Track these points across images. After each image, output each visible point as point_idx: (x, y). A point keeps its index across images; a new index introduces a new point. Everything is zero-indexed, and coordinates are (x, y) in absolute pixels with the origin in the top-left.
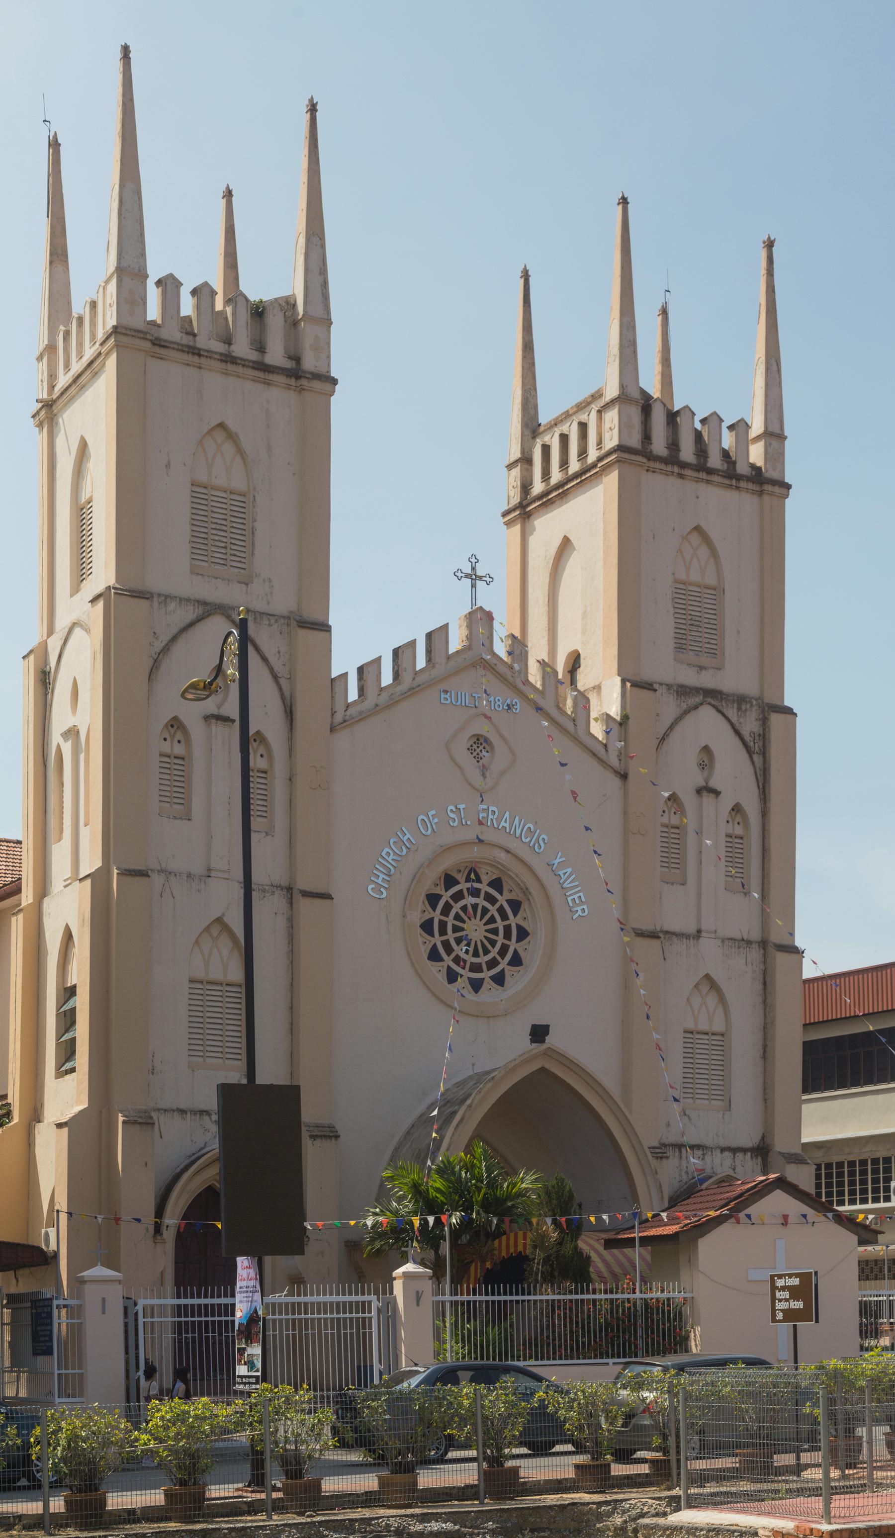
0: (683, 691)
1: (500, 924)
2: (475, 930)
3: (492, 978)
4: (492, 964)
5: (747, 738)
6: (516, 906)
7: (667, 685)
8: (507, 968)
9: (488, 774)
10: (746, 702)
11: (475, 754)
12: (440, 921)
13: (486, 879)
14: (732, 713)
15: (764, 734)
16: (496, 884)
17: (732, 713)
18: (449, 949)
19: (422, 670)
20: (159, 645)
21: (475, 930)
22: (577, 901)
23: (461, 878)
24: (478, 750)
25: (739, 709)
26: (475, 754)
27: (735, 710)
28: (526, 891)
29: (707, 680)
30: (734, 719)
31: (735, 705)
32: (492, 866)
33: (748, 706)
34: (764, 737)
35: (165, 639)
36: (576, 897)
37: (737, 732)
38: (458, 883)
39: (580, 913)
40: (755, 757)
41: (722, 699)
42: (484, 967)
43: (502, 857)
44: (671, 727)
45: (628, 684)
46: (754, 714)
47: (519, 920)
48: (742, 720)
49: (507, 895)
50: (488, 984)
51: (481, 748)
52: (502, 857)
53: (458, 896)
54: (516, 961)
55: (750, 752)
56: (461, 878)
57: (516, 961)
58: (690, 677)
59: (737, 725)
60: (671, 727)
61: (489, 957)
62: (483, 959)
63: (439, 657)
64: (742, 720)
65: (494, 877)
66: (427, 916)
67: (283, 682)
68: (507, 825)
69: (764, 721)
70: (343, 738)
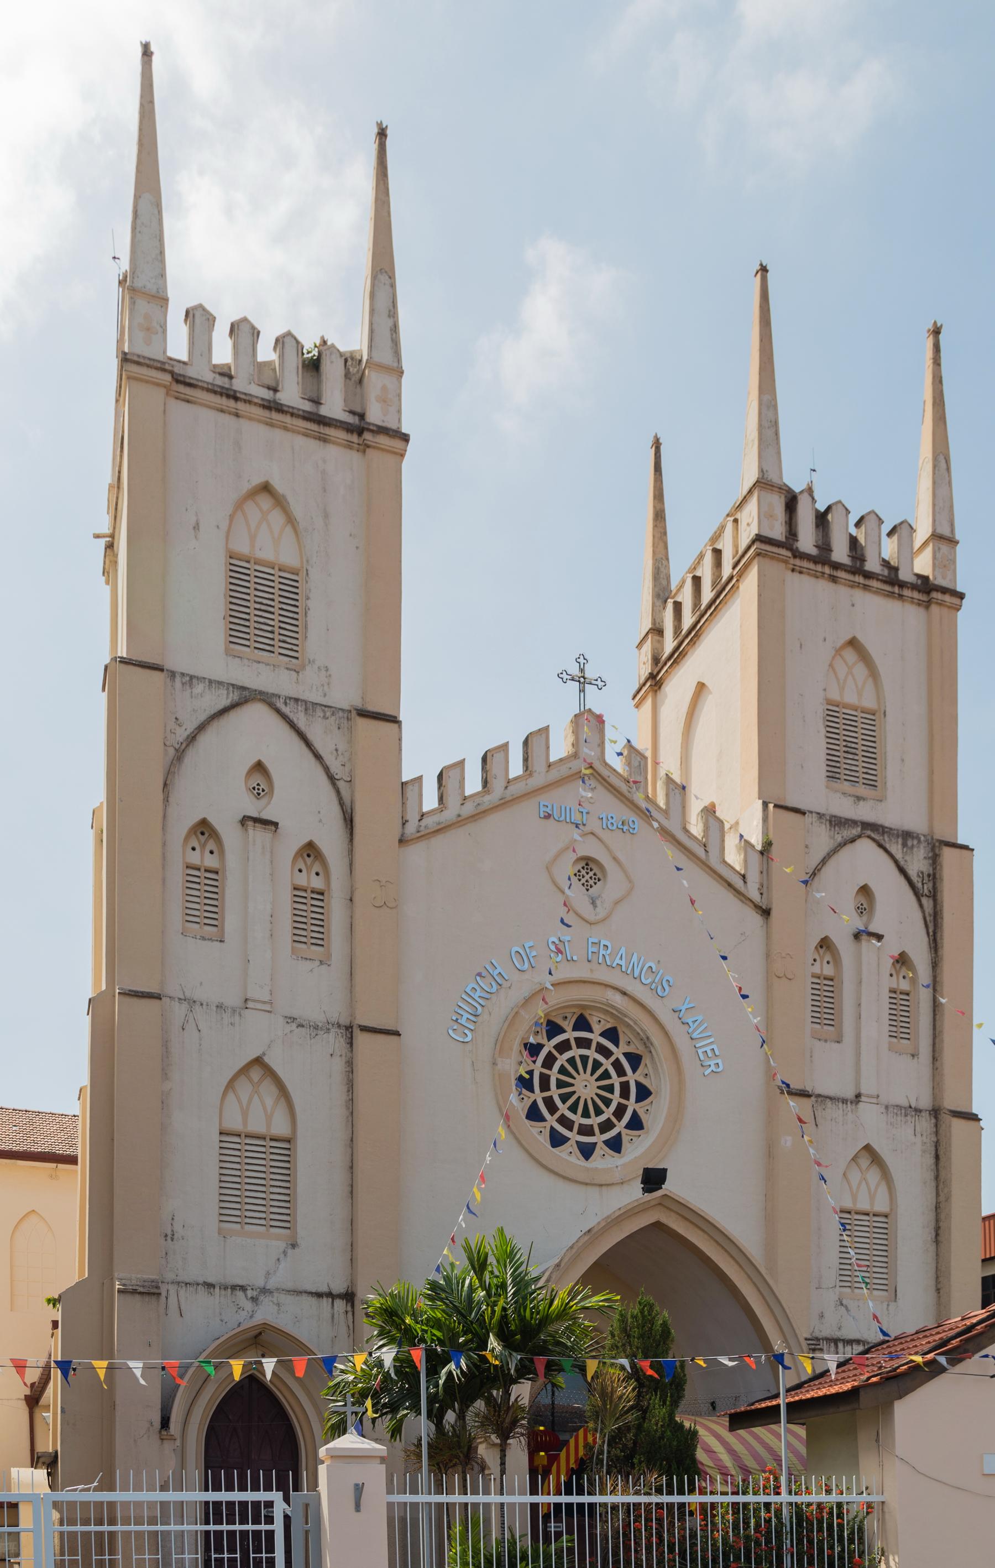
0: (837, 822)
1: (616, 1081)
3: (606, 1143)
4: (606, 1126)
5: (915, 878)
6: (635, 1060)
7: (818, 813)
8: (625, 1132)
9: (598, 902)
10: (913, 838)
11: (583, 881)
13: (598, 1029)
14: (896, 849)
15: (934, 874)
16: (611, 1034)
17: (896, 849)
19: (516, 779)
20: (182, 734)
22: (710, 1054)
23: (568, 1025)
24: (587, 877)
25: (904, 845)
26: (583, 881)
27: (900, 846)
28: (646, 1042)
29: (865, 812)
30: (899, 856)
31: (900, 840)
32: (606, 1012)
33: (915, 842)
34: (934, 878)
35: (190, 726)
36: (708, 1049)
37: (902, 871)
38: (563, 1031)
39: (713, 1068)
40: (924, 901)
41: (883, 833)
42: (597, 1130)
43: (617, 1000)
44: (824, 861)
45: (771, 806)
46: (922, 851)
47: (639, 1076)
48: (907, 858)
49: (624, 1048)
50: (601, 1149)
51: (591, 874)
52: (617, 1000)
53: (564, 1047)
54: (636, 1124)
55: (918, 895)
56: (568, 1025)
57: (636, 1124)
58: (845, 808)
59: (902, 863)
60: (824, 861)
62: (594, 1121)
63: (538, 765)
64: (907, 858)
65: (609, 1026)
67: (341, 784)
68: (623, 963)
69: (935, 859)
70: (416, 854)
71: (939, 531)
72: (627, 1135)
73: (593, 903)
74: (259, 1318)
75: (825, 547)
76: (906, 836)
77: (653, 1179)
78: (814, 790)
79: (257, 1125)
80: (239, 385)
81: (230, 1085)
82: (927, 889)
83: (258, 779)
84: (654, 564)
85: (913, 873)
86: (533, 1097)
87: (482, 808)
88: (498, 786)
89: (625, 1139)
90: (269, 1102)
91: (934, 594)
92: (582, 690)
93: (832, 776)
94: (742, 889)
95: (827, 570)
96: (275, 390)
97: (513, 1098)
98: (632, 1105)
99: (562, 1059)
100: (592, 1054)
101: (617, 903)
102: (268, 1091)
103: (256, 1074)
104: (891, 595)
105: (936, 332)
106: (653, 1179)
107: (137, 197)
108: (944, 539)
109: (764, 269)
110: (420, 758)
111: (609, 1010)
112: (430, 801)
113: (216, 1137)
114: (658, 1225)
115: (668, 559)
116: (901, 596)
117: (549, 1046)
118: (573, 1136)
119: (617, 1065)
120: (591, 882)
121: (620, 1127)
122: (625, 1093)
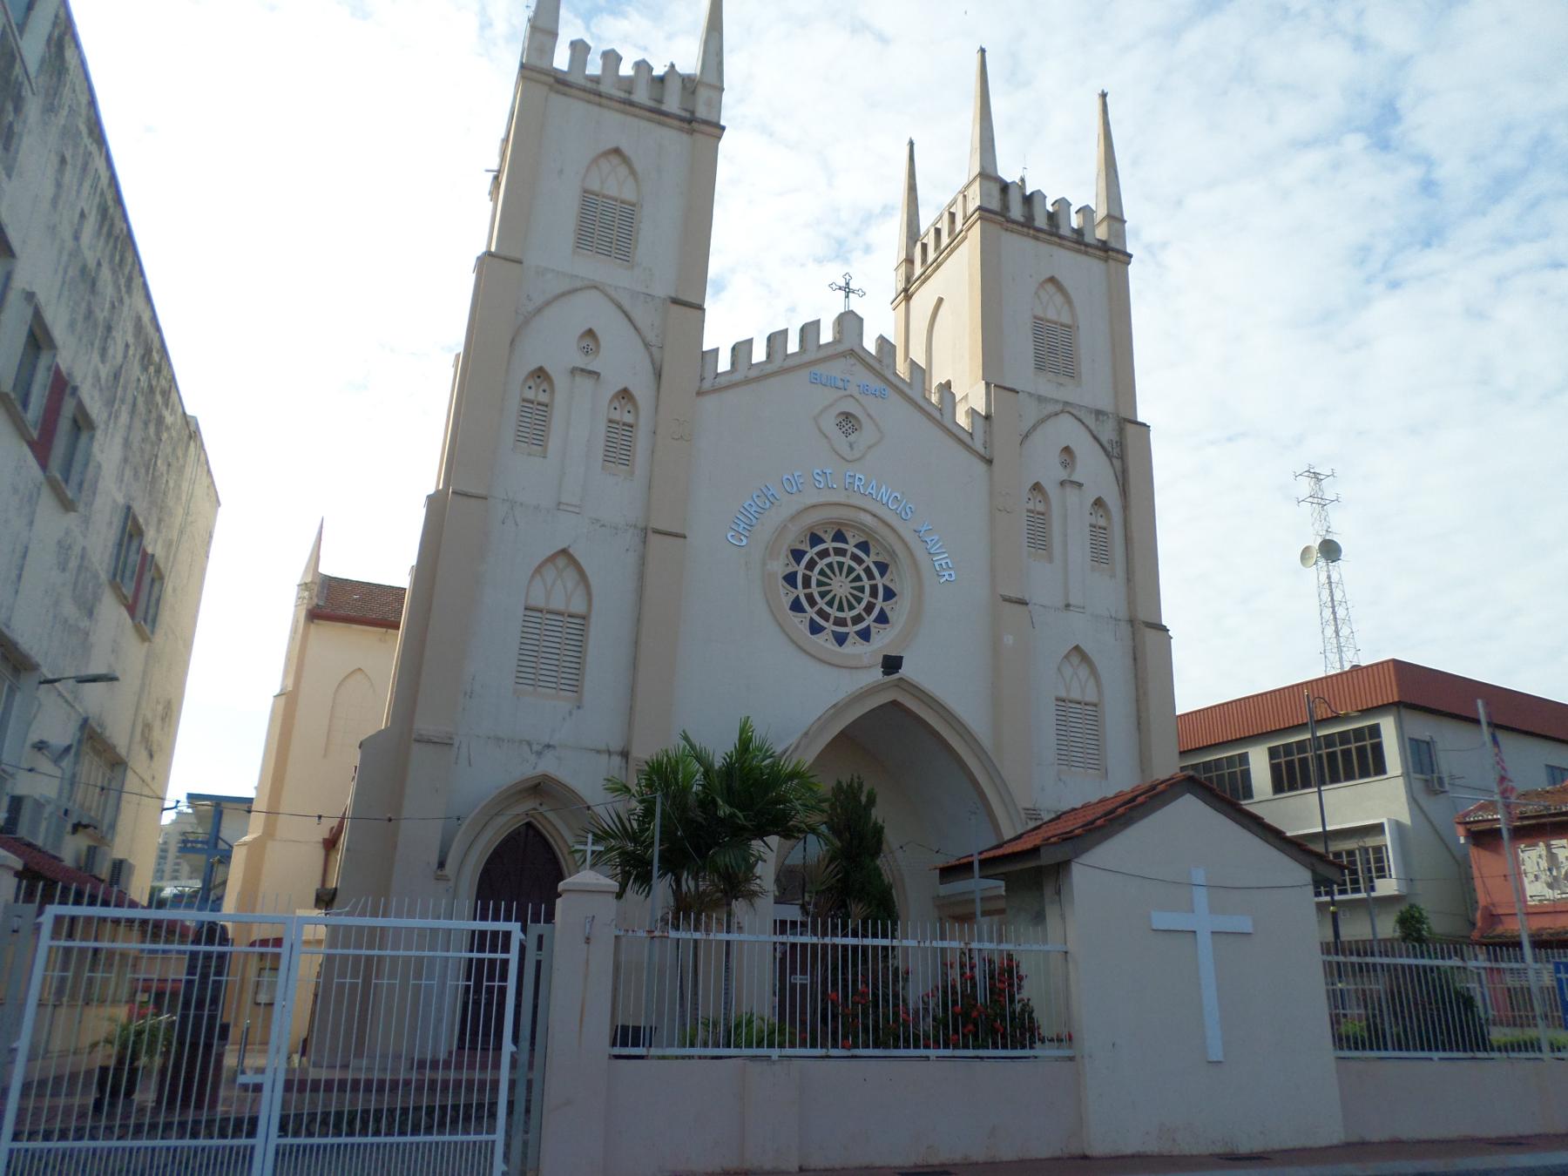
1: (866, 583)
2: (841, 587)
3: (858, 633)
4: (858, 619)
6: (883, 568)
12: (805, 576)
16: (864, 546)
23: (828, 537)
28: (893, 554)
30: (1093, 427)
37: (1096, 438)
44: (1034, 427)
47: (886, 580)
49: (873, 557)
50: (853, 638)
52: (868, 519)
53: (824, 554)
54: (883, 619)
56: (828, 537)
57: (883, 619)
60: (1034, 427)
66: (790, 569)
69: (1121, 431)
70: (710, 402)
73: (851, 446)
74: (540, 770)
76: (1099, 413)
77: (892, 664)
79: (558, 603)
80: (603, 88)
81: (539, 570)
82: (1116, 452)
83: (588, 341)
85: (1104, 440)
86: (796, 592)
90: (570, 585)
93: (1040, 367)
96: (630, 93)
97: (782, 592)
98: (879, 603)
101: (870, 447)
102: (571, 576)
103: (561, 562)
111: (861, 527)
113: (520, 612)
117: (811, 553)
118: (829, 626)
119: (868, 571)
122: (874, 593)
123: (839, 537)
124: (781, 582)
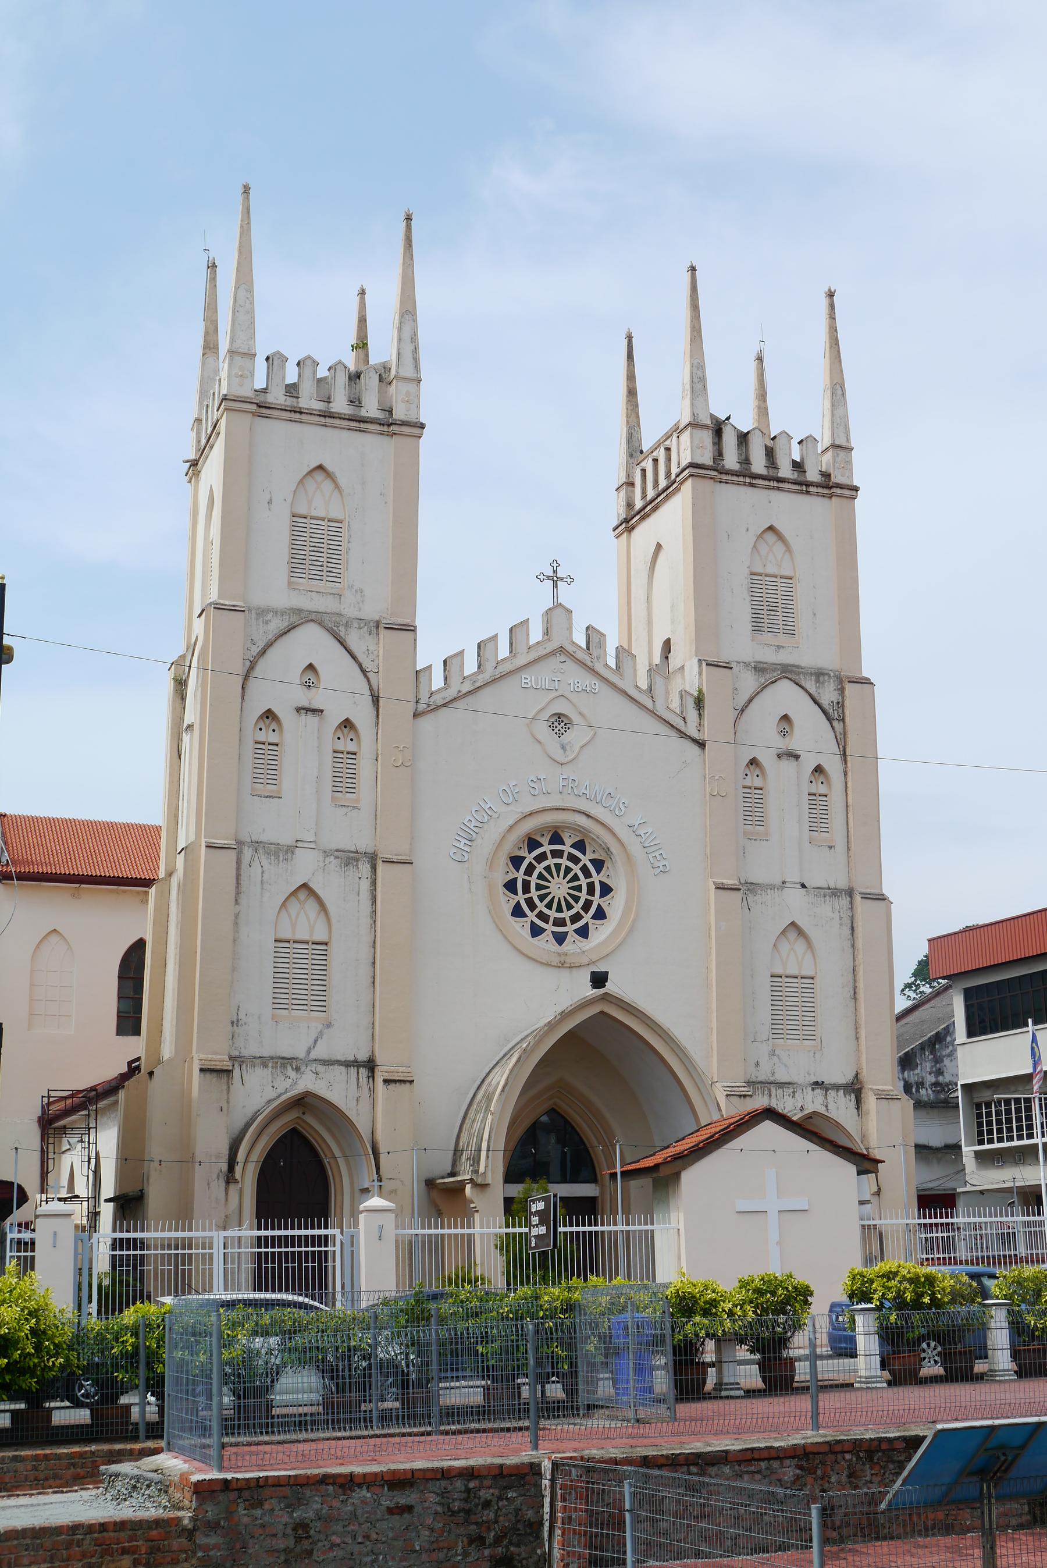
0: (759, 668)
1: (583, 882)
2: (559, 888)
3: (576, 931)
5: (826, 706)
6: (599, 864)
8: (591, 922)
9: (568, 748)
11: (556, 730)
13: (569, 842)
15: (843, 702)
16: (580, 846)
17: (811, 685)
18: (532, 905)
19: (503, 660)
20: (255, 650)
21: (559, 888)
22: (659, 858)
23: (544, 841)
24: (559, 727)
26: (556, 730)
28: (608, 850)
29: (784, 657)
30: (812, 691)
32: (575, 829)
33: (826, 678)
34: (843, 705)
35: (261, 644)
39: (661, 868)
40: (835, 723)
43: (582, 821)
44: (750, 700)
45: (704, 664)
46: (832, 684)
47: (602, 877)
48: (820, 691)
49: (590, 855)
50: (572, 936)
51: (562, 724)
52: (582, 821)
53: (541, 858)
54: (600, 914)
55: (830, 719)
56: (544, 841)
57: (600, 914)
58: (769, 656)
59: (816, 695)
60: (750, 700)
61: (573, 912)
62: (566, 914)
63: (521, 648)
64: (820, 691)
66: (511, 877)
67: (371, 675)
68: (587, 792)
69: (842, 691)
70: (427, 723)
71: (837, 443)
72: (604, 902)
73: (563, 748)
75: (746, 461)
78: (742, 645)
83: (310, 675)
84: (628, 431)
87: (478, 684)
88: (489, 667)
89: (604, 906)
91: (834, 488)
92: (555, 586)
93: (758, 628)
94: (683, 729)
95: (748, 480)
97: (503, 899)
98: (596, 900)
99: (540, 868)
100: (564, 862)
104: (800, 492)
105: (831, 295)
106: (599, 980)
107: (237, 288)
108: (841, 448)
109: (693, 269)
110: (430, 652)
111: (576, 829)
112: (438, 682)
114: (602, 1012)
115: (639, 426)
116: (808, 492)
117: (530, 858)
118: (549, 927)
120: (562, 731)
121: (587, 918)
122: (591, 890)
123: (556, 839)
124: (502, 890)
